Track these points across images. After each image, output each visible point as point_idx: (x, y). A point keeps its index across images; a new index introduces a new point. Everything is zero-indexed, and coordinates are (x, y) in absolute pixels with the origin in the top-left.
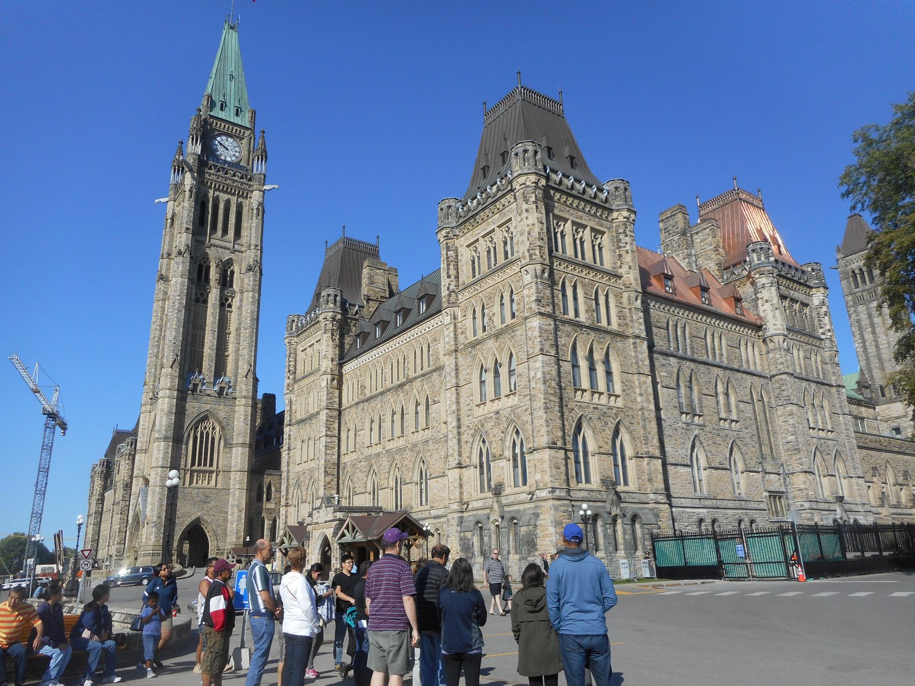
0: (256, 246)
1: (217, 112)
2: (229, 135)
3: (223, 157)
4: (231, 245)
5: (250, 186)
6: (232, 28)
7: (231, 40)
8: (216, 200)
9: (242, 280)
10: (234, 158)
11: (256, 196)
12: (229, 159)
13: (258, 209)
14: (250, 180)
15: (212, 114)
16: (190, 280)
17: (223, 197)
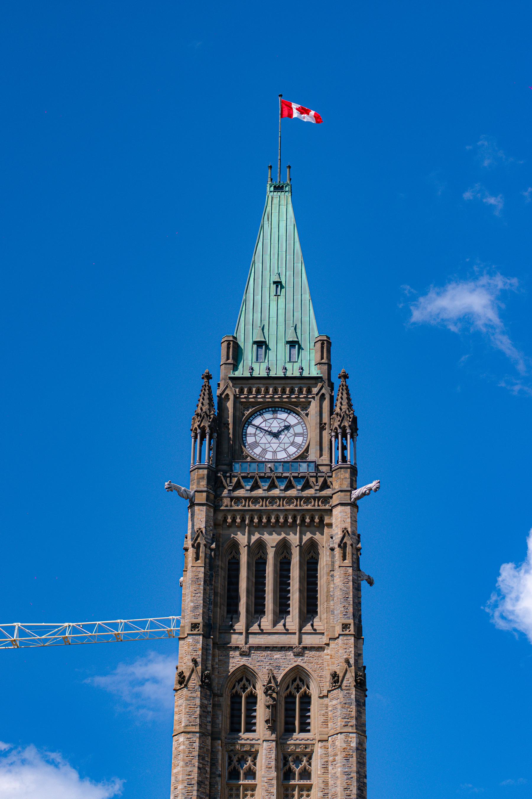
0: (345, 626)
1: (251, 365)
2: (275, 407)
3: (269, 456)
4: (293, 640)
5: (326, 499)
6: (278, 188)
7: (280, 215)
8: (258, 550)
9: (328, 714)
10: (292, 450)
11: (340, 518)
12: (281, 456)
13: (342, 546)
14: (325, 486)
15: (238, 374)
16: (203, 735)
17: (272, 540)
